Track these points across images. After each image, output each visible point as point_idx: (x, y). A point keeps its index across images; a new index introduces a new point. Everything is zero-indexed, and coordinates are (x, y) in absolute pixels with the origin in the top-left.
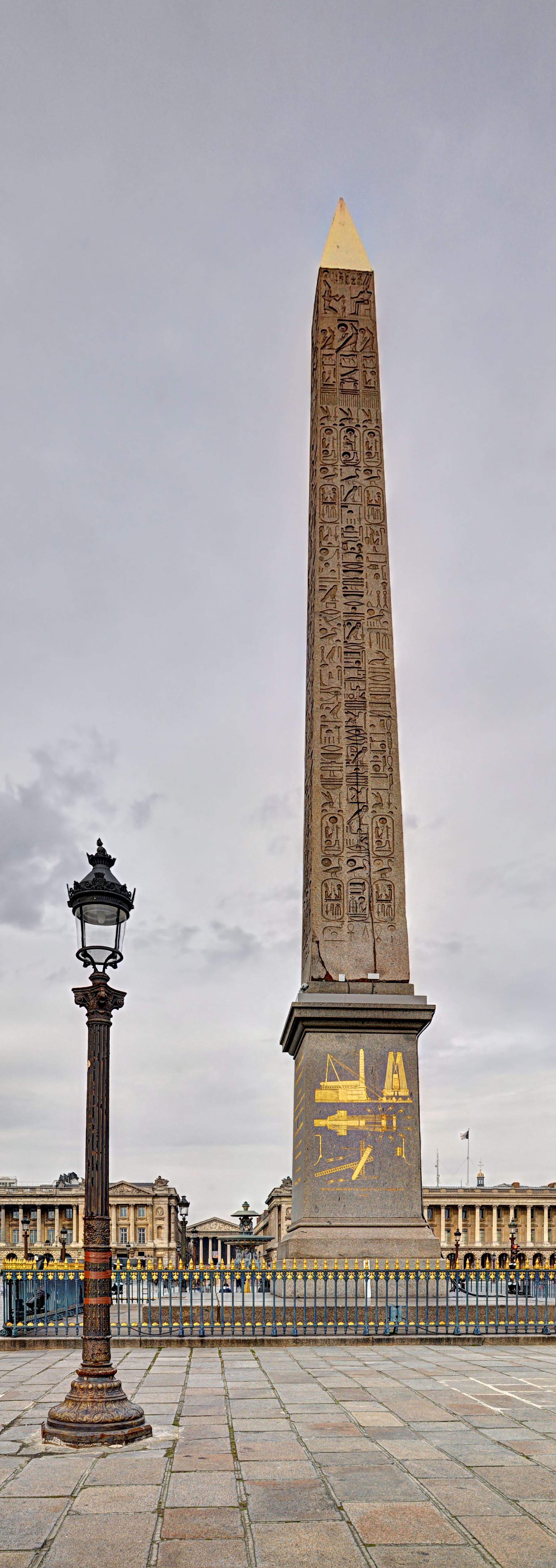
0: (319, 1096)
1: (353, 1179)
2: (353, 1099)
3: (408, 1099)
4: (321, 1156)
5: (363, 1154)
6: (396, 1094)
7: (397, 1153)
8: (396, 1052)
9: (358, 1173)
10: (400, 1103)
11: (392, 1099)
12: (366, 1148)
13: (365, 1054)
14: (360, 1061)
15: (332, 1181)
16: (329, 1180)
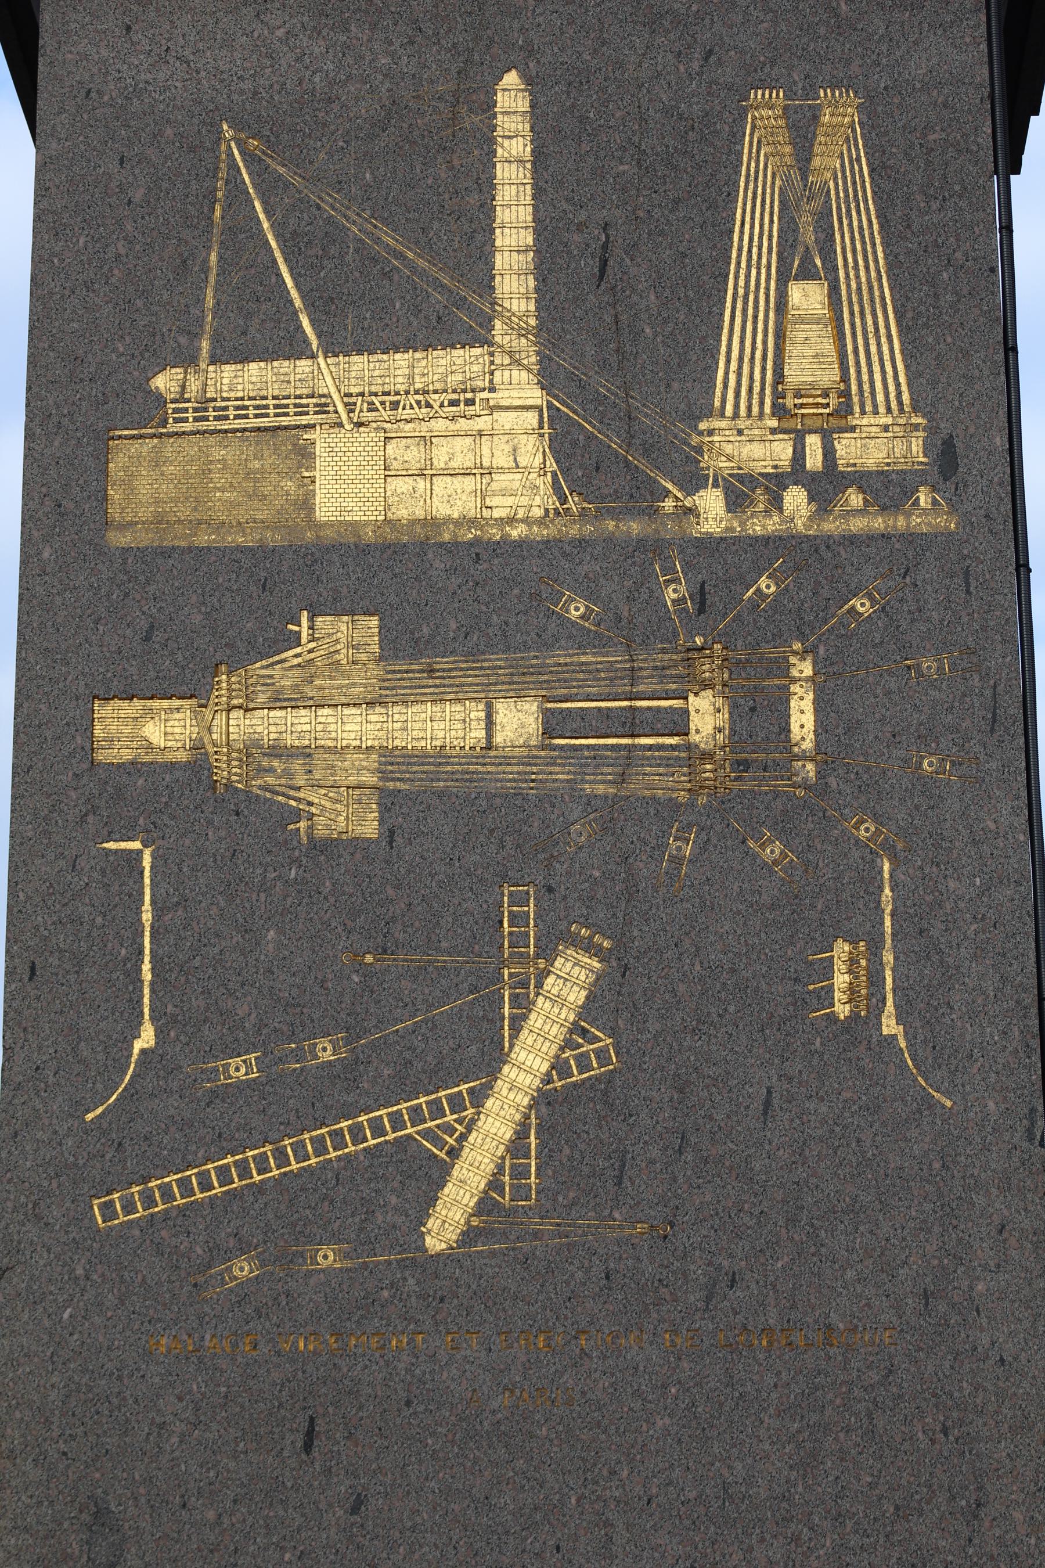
0: (144, 489)
1: (434, 1244)
2: (442, 509)
3: (924, 498)
4: (146, 1038)
5: (523, 1005)
6: (814, 460)
7: (826, 996)
8: (810, 92)
9: (478, 1182)
10: (851, 540)
11: (776, 503)
12: (547, 952)
13: (536, 114)
14: (502, 172)
15: (243, 1269)
16: (224, 1254)
